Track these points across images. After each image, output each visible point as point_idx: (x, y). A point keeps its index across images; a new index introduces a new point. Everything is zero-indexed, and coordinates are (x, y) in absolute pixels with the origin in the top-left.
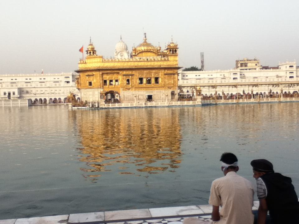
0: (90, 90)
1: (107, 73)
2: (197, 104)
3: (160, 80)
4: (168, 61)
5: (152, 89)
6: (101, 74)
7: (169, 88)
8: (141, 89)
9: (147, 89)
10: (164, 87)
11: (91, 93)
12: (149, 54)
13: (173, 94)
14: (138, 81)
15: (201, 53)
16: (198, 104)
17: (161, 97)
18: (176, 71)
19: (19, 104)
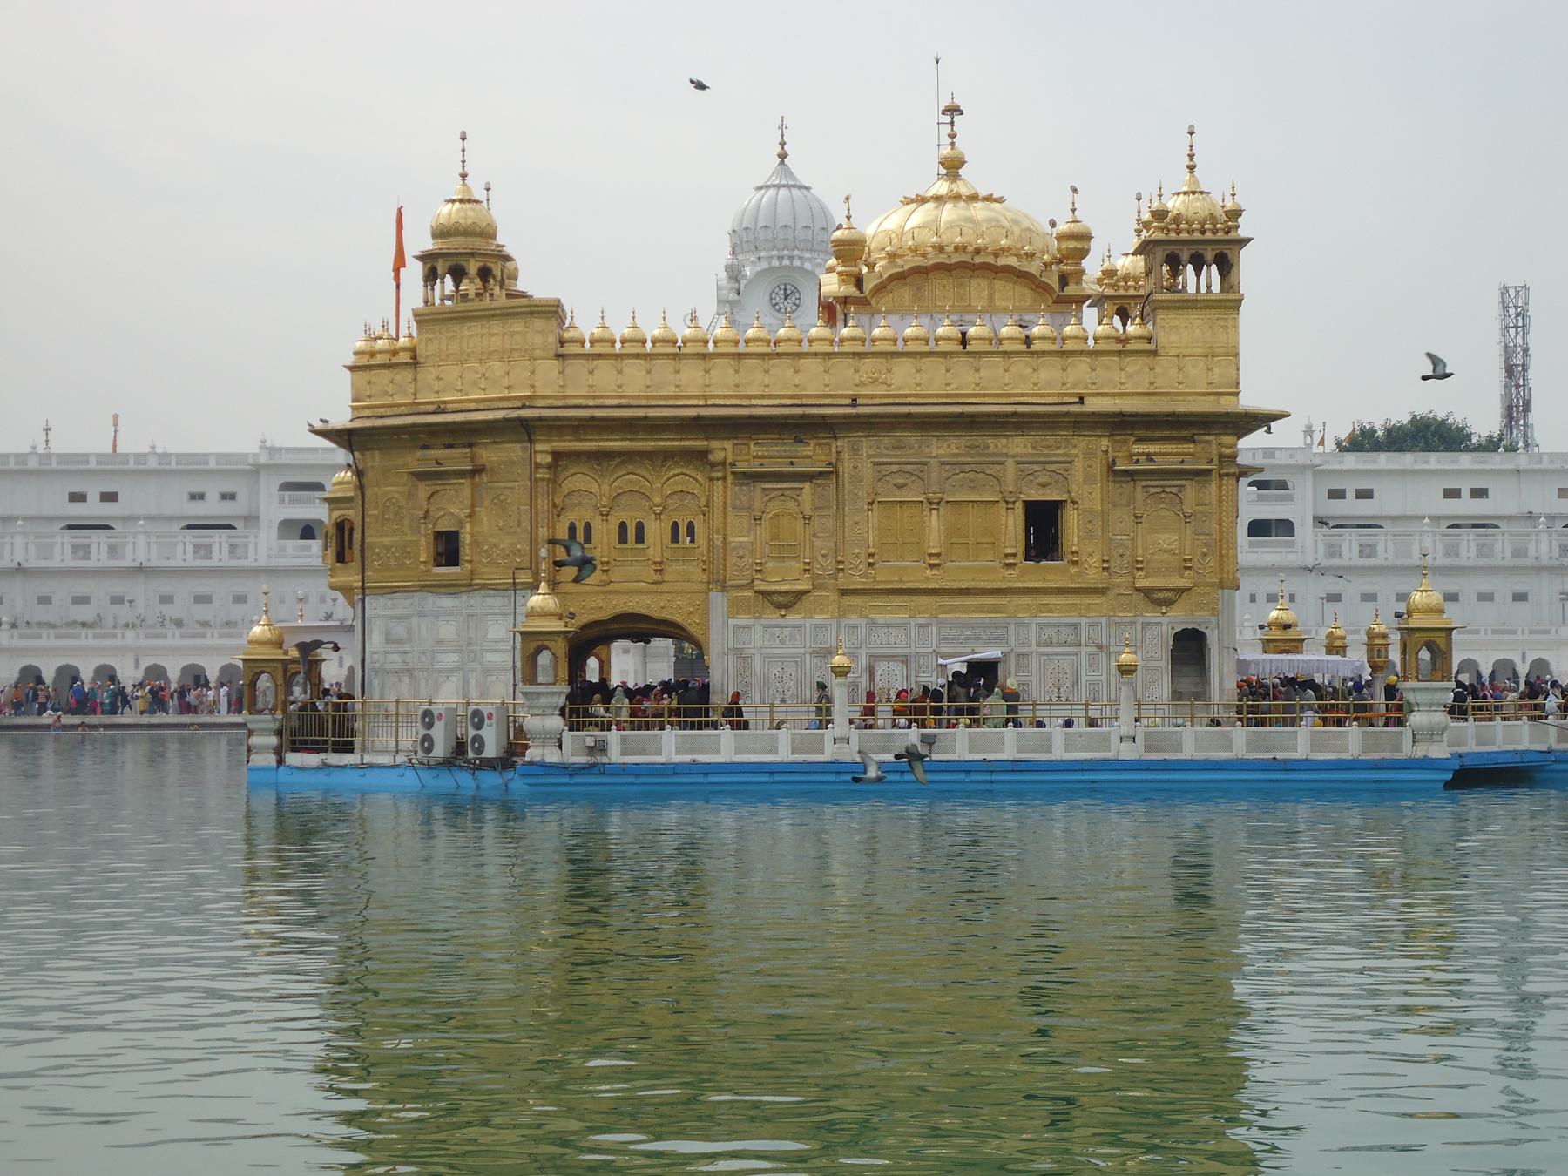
0: (447, 602)
2: (1407, 750)
3: (1072, 524)
4: (1154, 353)
5: (996, 609)
6: (548, 459)
7: (1158, 599)
9: (947, 601)
10: (1101, 591)
11: (447, 630)
12: (978, 289)
13: (1190, 649)
15: (1506, 288)
16: (1421, 751)
17: (1076, 682)
18: (1214, 443)
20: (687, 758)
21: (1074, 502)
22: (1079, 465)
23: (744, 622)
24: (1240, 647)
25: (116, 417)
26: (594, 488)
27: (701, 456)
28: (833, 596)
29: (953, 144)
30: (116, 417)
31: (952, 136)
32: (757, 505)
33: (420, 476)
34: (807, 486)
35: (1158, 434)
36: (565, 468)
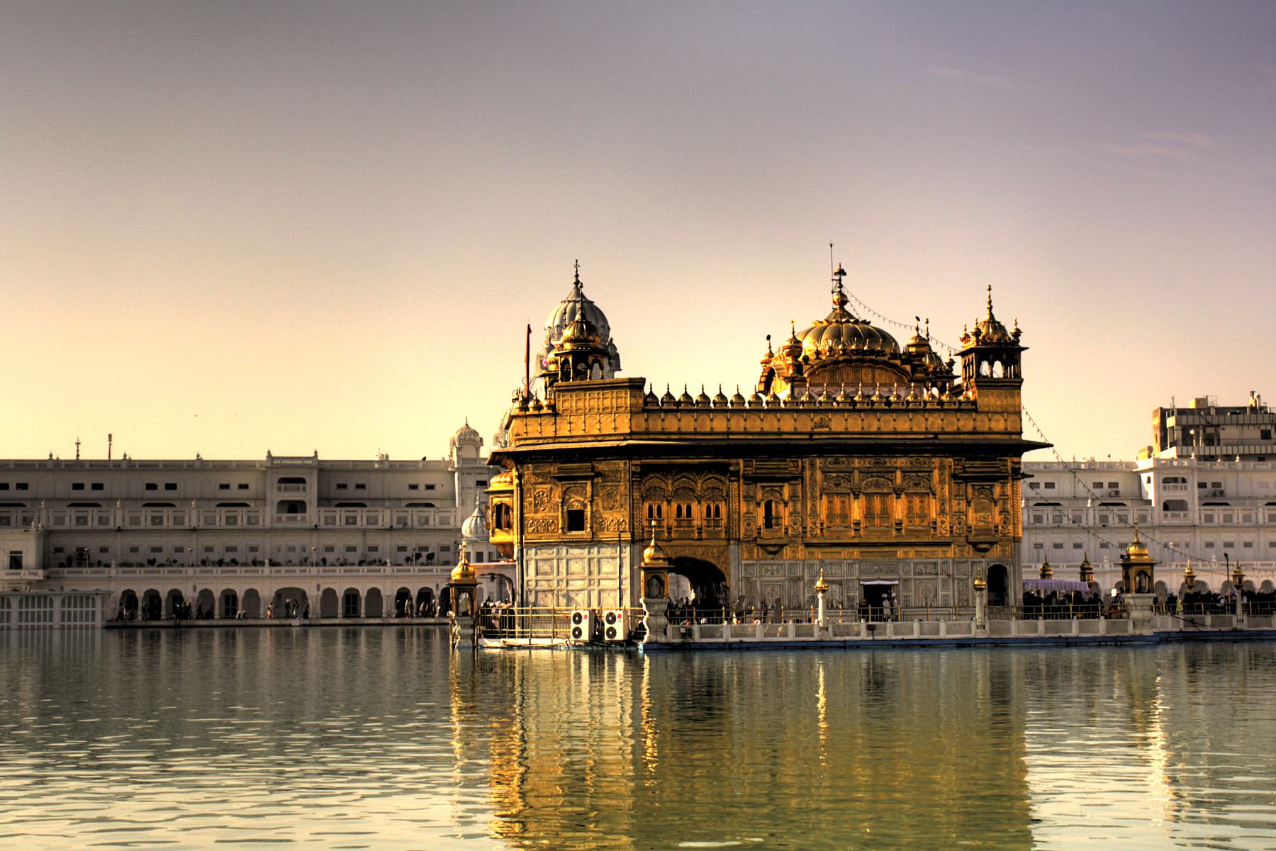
1: (667, 470)
2: (1131, 631)
8: (835, 549)
9: (864, 549)
10: (948, 544)
12: (866, 374)
13: (997, 579)
16: (1138, 632)
17: (936, 595)
18: (1009, 462)
19: (57, 616)
20: (737, 640)
22: (936, 473)
24: (1027, 575)
25: (110, 436)
26: (664, 485)
28: (801, 547)
30: (110, 436)
31: (841, 286)
32: (759, 496)
33: (560, 479)
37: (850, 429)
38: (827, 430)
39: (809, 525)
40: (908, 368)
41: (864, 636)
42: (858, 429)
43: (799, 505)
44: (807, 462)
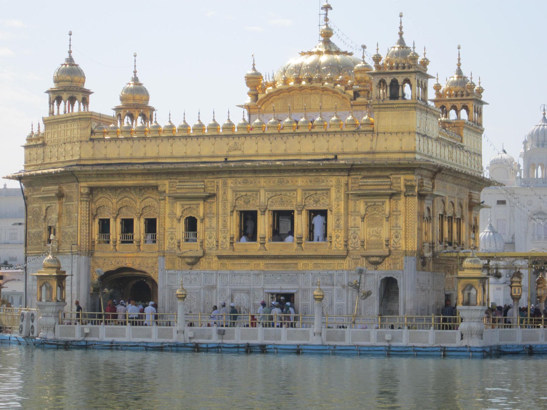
2: (458, 343)
6: (86, 191)
8: (244, 261)
10: (343, 257)
12: (314, 100)
14: (233, 224)
16: (464, 343)
17: (331, 304)
18: (401, 180)
20: (110, 339)
21: (331, 211)
23: (173, 272)
27: (156, 187)
28: (216, 259)
29: (327, 25)
31: (326, 19)
34: (201, 202)
35: (373, 174)
36: (97, 194)
37: (260, 152)
38: (239, 153)
39: (221, 239)
40: (351, 93)
41: (215, 340)
42: (267, 152)
43: (214, 220)
44: (220, 181)
